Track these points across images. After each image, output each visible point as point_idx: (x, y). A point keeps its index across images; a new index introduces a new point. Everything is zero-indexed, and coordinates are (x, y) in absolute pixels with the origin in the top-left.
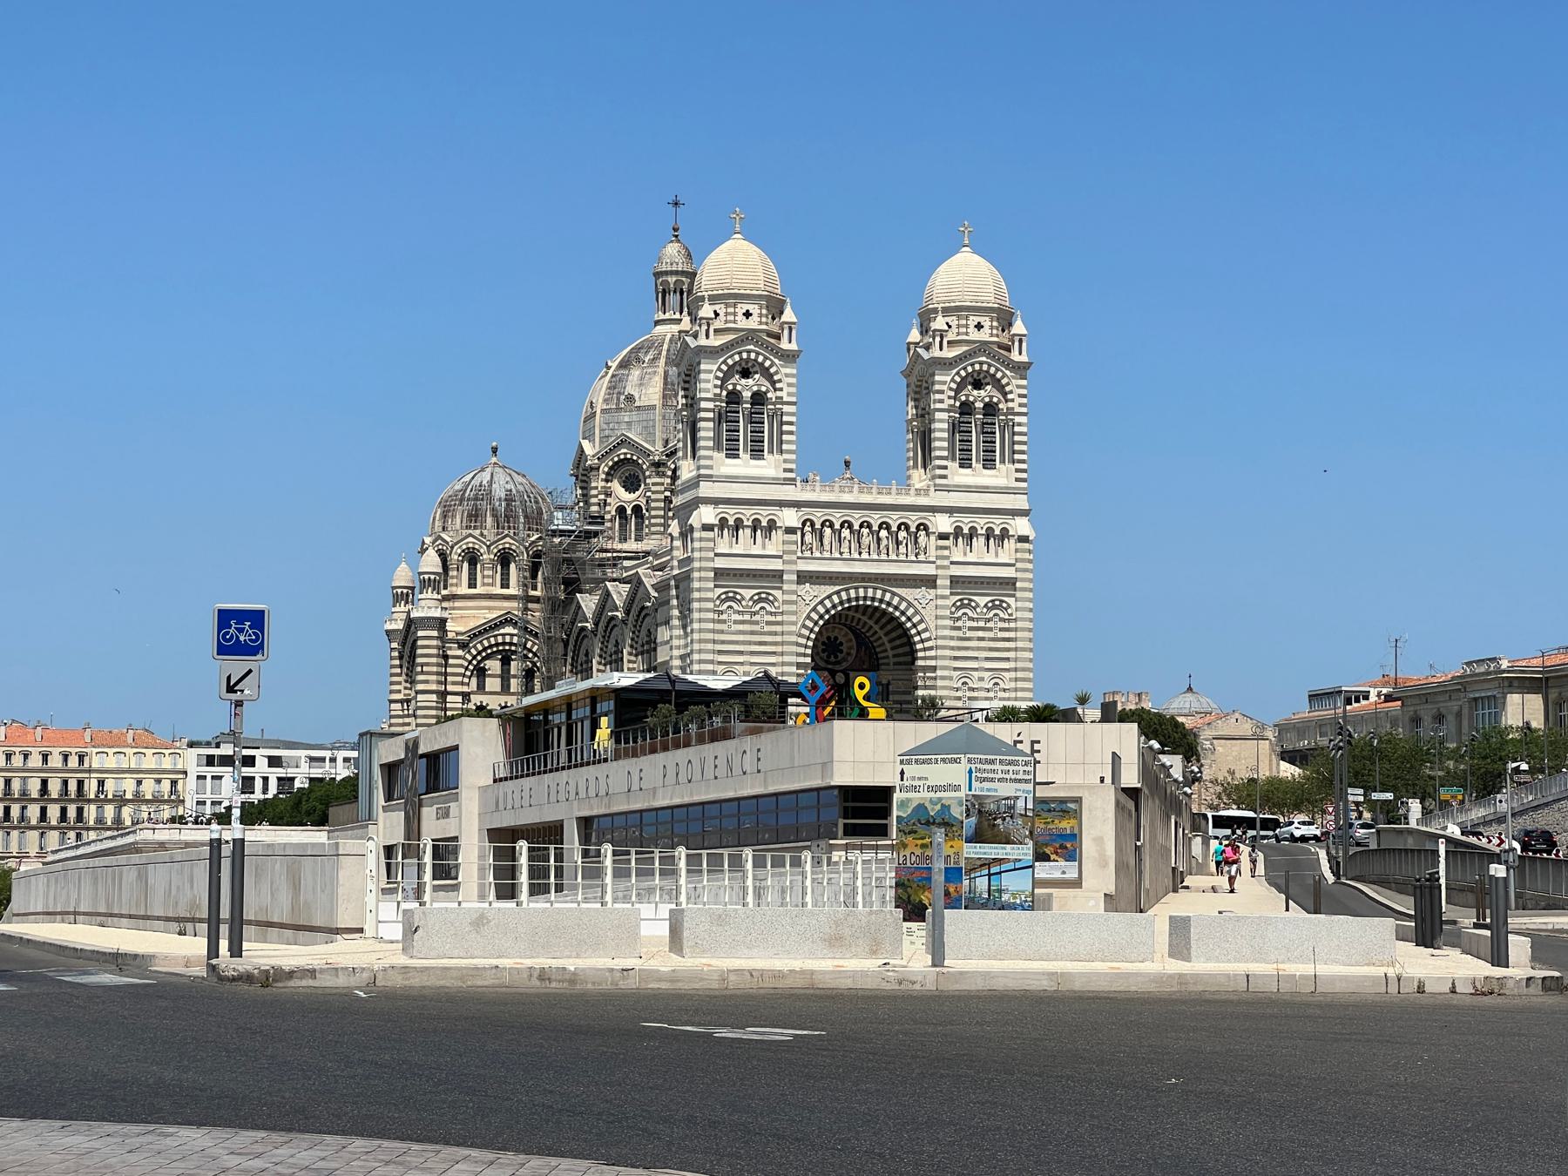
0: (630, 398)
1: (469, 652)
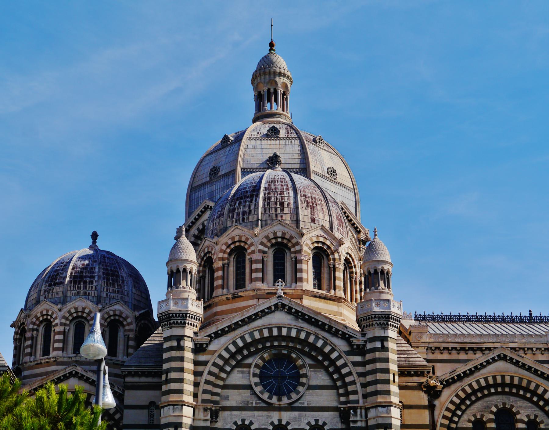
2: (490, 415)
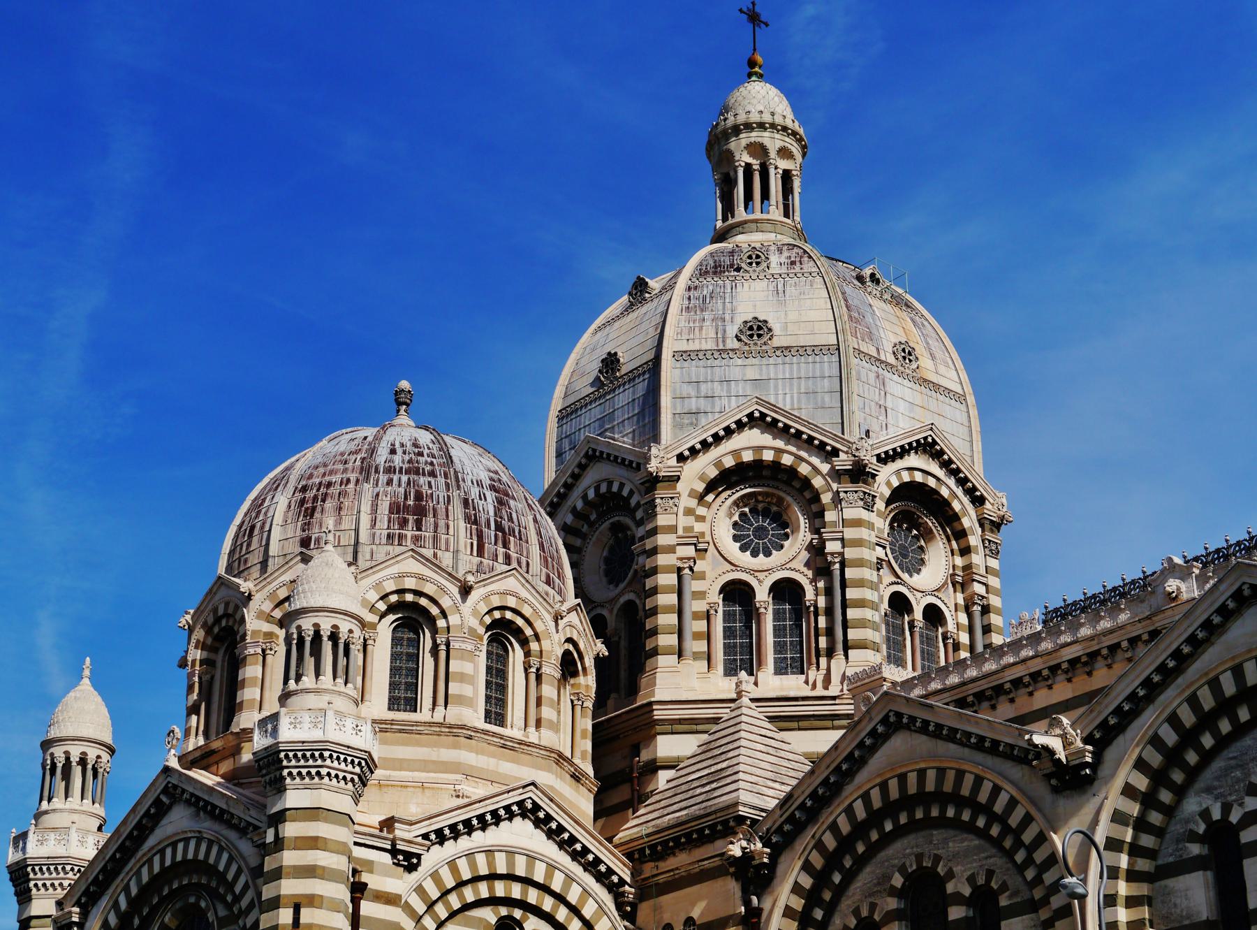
0: (757, 329)
1: (420, 890)
2: (890, 900)
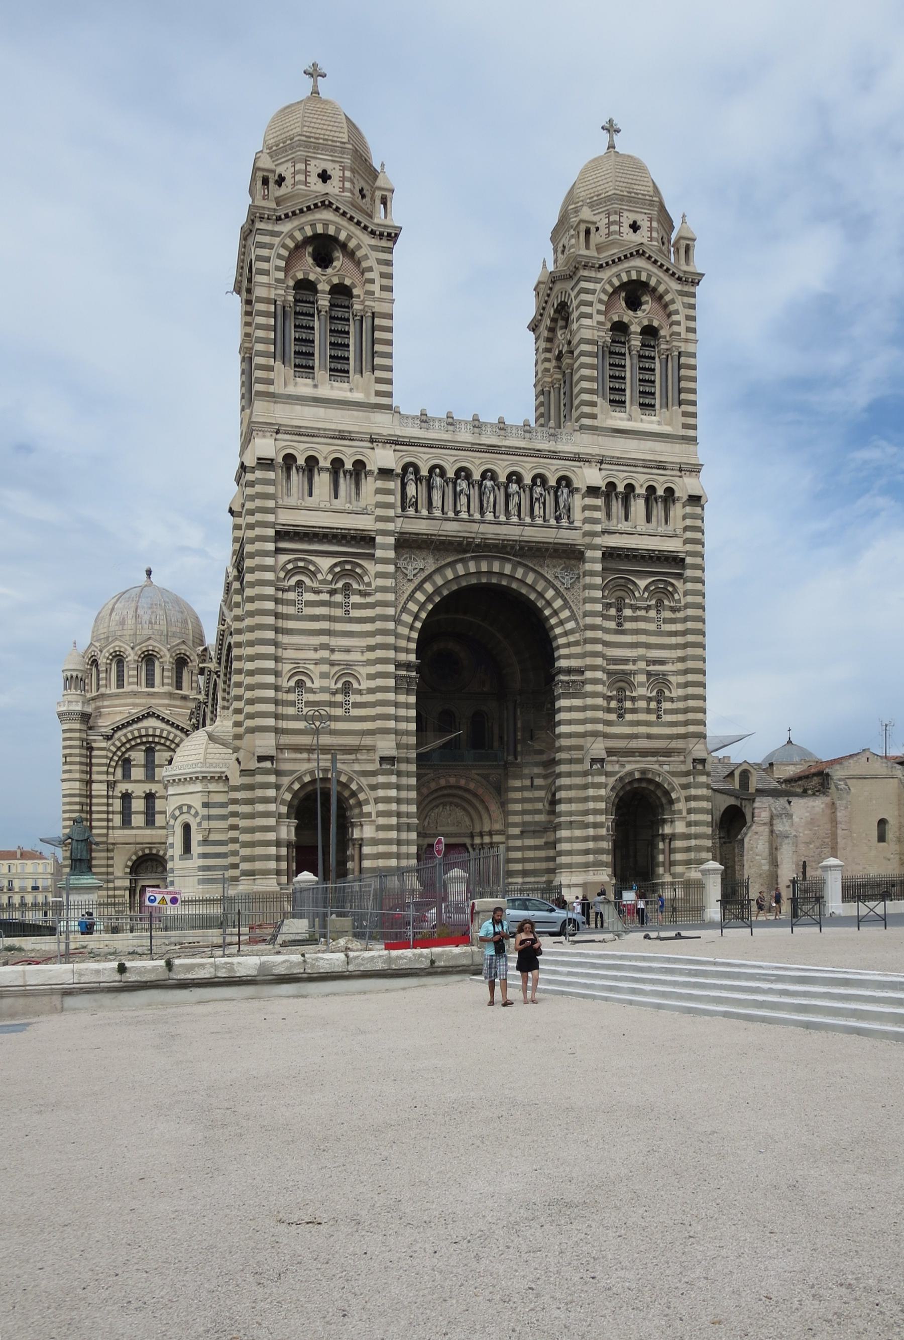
1: (114, 744)
